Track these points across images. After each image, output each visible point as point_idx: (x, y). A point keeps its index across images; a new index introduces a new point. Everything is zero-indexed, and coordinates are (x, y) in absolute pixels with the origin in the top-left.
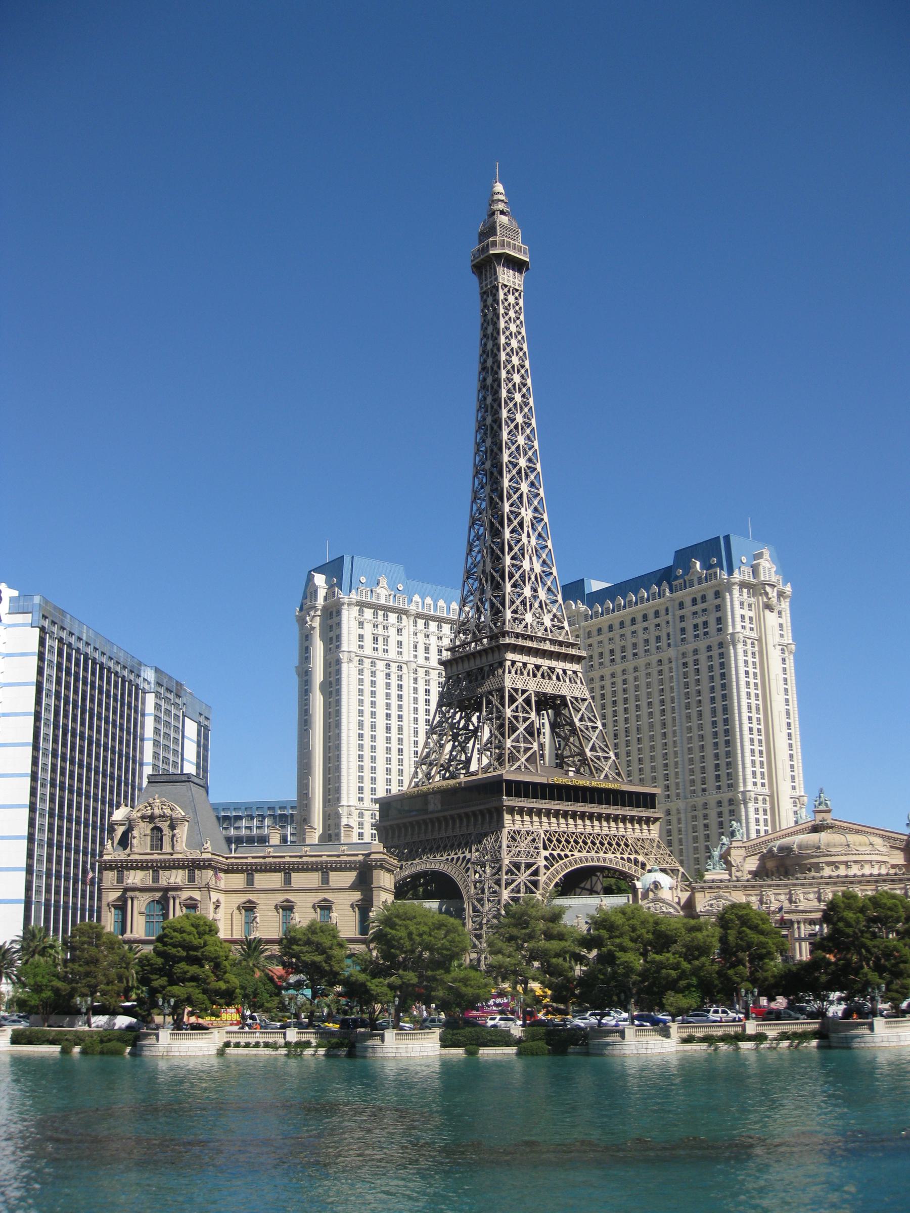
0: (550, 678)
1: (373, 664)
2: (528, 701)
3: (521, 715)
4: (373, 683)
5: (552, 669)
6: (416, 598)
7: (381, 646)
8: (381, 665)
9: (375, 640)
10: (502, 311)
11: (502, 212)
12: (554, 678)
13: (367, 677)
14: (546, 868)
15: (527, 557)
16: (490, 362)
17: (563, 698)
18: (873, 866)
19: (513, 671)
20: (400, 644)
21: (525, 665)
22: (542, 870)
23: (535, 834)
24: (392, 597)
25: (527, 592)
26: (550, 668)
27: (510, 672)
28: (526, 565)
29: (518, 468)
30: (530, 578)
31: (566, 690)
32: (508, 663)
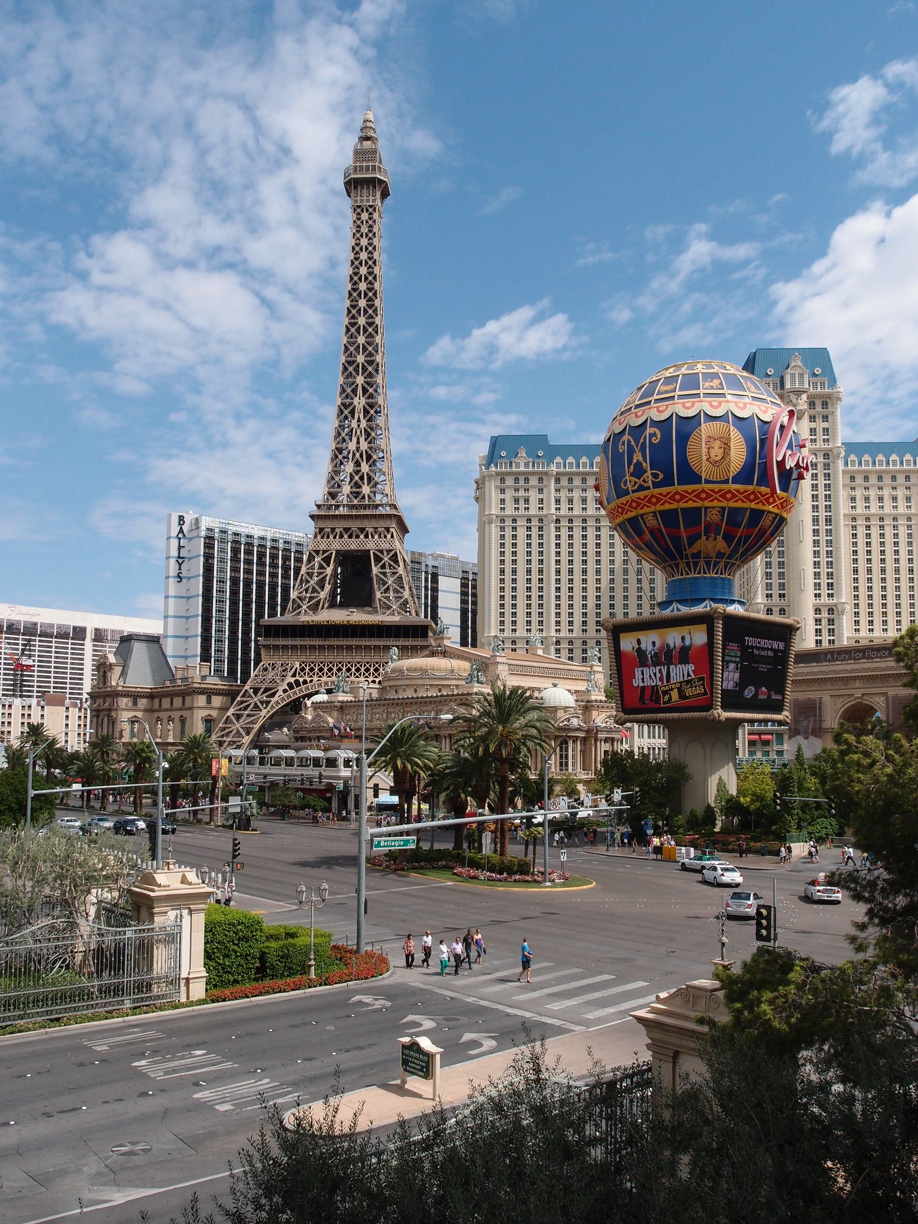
0: (358, 537)
2: (327, 560)
4: (514, 537)
5: (362, 530)
6: (558, 459)
7: (522, 505)
8: (521, 523)
12: (362, 536)
13: (508, 533)
14: (285, 691)
15: (354, 439)
18: (440, 690)
20: (541, 501)
21: (333, 530)
22: (280, 693)
24: (531, 464)
25: (349, 467)
28: (352, 446)
30: (354, 454)
31: (371, 545)
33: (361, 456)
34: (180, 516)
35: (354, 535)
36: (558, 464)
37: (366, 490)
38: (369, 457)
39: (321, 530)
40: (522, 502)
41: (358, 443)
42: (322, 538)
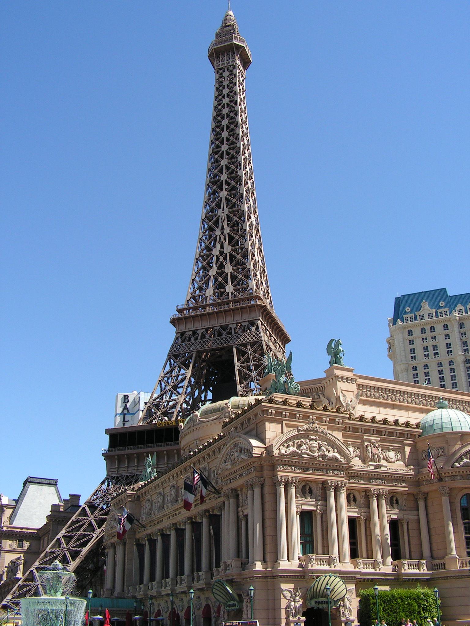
0: (220, 334)
1: (426, 367)
5: (224, 328)
7: (431, 352)
9: (426, 349)
12: (224, 333)
20: (449, 345)
21: (194, 332)
25: (213, 272)
26: (221, 327)
28: (216, 251)
33: (225, 259)
34: (125, 396)
36: (460, 311)
37: (229, 288)
38: (232, 258)
39: (182, 334)
40: (430, 349)
41: (222, 247)
42: (183, 341)
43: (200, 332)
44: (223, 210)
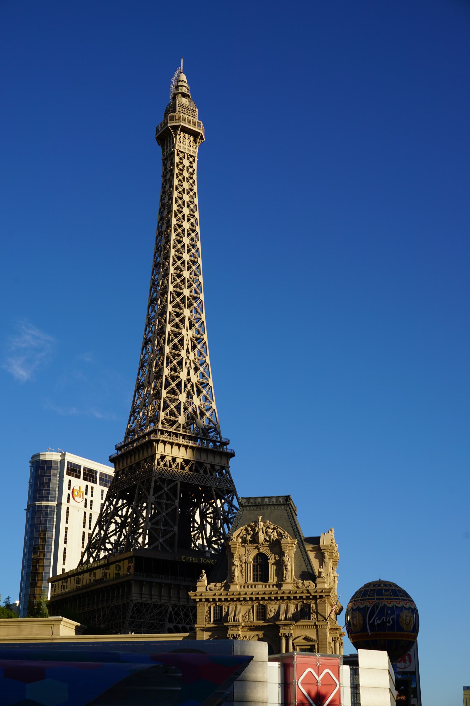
0: (198, 471)
2: (173, 491)
3: (165, 501)
10: (176, 171)
11: (184, 95)
12: (202, 471)
15: (185, 370)
16: (165, 214)
17: (210, 487)
19: (162, 464)
21: (174, 459)
23: (163, 608)
25: (182, 398)
27: (159, 464)
28: (183, 376)
29: (181, 297)
30: (186, 386)
32: (158, 457)
35: (194, 468)
41: (188, 374)
42: (165, 465)
43: (179, 461)
44: (187, 331)
